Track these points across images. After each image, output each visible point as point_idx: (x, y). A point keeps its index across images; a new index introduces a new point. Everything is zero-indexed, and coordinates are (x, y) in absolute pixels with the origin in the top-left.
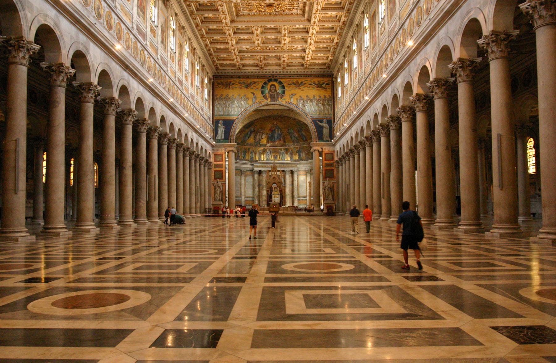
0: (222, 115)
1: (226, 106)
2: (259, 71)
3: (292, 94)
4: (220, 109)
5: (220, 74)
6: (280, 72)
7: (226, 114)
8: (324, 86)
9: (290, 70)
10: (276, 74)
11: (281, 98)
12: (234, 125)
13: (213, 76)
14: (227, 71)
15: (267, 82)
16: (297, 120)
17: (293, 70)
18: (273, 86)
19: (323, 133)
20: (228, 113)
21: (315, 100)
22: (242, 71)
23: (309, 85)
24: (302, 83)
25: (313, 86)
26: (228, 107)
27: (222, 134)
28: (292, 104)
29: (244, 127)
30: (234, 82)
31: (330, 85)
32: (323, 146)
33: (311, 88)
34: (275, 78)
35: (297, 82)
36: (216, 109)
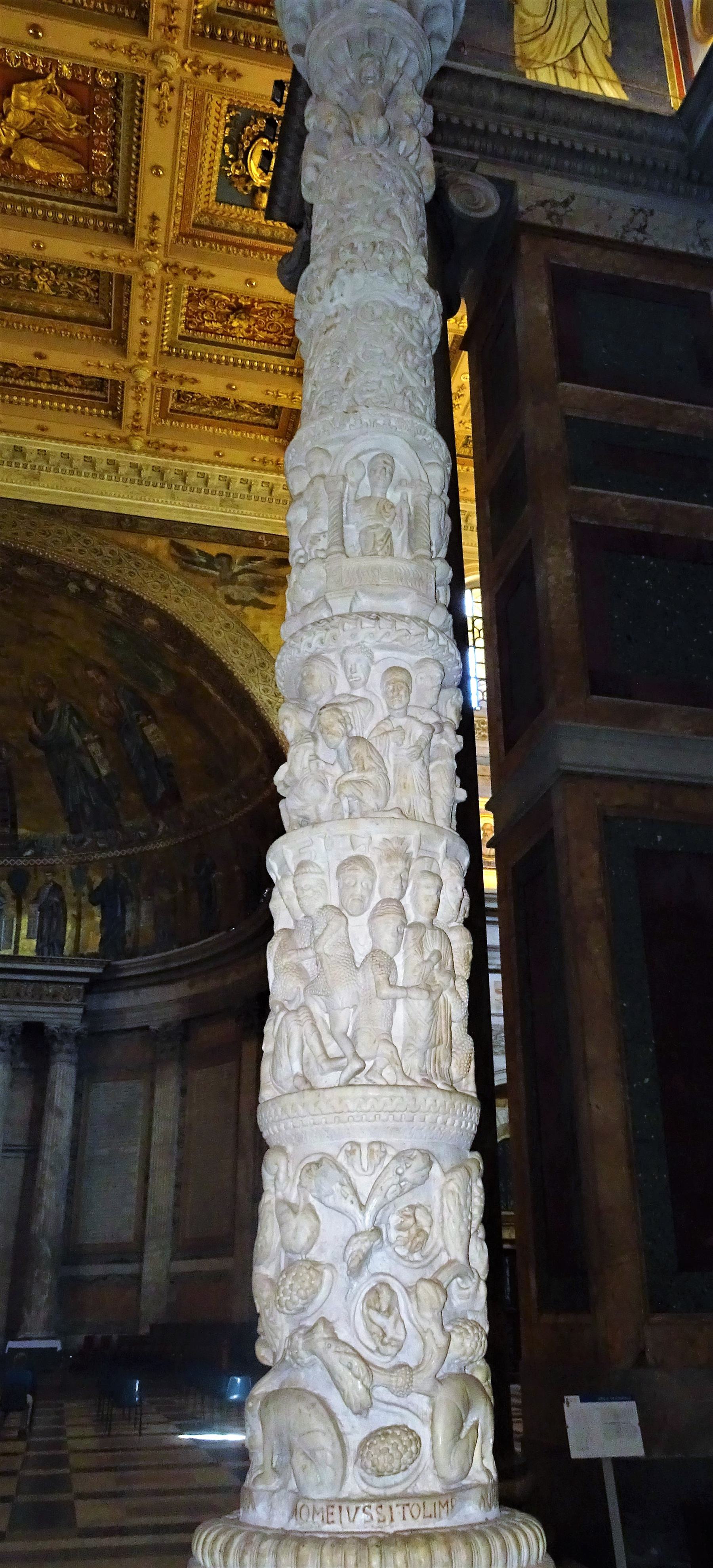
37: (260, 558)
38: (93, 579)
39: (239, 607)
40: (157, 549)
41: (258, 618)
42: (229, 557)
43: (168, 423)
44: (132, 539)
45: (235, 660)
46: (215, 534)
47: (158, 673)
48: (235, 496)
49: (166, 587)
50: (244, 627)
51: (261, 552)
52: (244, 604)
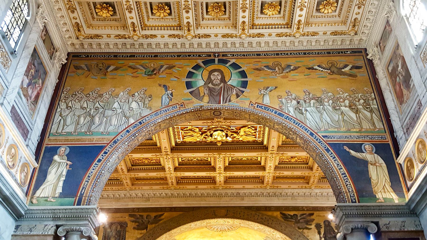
0: (70, 134)
7: (83, 131)
8: (347, 69)
11: (238, 96)
12: (100, 157)
13: (69, 54)
15: (202, 64)
18: (216, 73)
20: (90, 126)
22: (142, 40)
24: (289, 66)
27: (59, 179)
28: (267, 108)
30: (119, 66)
33: (313, 74)
34: (221, 58)
36: (57, 118)
37: (305, 214)
40: (277, 215)
42: (297, 215)
44: (270, 213)
48: (295, 196)
51: (305, 212)
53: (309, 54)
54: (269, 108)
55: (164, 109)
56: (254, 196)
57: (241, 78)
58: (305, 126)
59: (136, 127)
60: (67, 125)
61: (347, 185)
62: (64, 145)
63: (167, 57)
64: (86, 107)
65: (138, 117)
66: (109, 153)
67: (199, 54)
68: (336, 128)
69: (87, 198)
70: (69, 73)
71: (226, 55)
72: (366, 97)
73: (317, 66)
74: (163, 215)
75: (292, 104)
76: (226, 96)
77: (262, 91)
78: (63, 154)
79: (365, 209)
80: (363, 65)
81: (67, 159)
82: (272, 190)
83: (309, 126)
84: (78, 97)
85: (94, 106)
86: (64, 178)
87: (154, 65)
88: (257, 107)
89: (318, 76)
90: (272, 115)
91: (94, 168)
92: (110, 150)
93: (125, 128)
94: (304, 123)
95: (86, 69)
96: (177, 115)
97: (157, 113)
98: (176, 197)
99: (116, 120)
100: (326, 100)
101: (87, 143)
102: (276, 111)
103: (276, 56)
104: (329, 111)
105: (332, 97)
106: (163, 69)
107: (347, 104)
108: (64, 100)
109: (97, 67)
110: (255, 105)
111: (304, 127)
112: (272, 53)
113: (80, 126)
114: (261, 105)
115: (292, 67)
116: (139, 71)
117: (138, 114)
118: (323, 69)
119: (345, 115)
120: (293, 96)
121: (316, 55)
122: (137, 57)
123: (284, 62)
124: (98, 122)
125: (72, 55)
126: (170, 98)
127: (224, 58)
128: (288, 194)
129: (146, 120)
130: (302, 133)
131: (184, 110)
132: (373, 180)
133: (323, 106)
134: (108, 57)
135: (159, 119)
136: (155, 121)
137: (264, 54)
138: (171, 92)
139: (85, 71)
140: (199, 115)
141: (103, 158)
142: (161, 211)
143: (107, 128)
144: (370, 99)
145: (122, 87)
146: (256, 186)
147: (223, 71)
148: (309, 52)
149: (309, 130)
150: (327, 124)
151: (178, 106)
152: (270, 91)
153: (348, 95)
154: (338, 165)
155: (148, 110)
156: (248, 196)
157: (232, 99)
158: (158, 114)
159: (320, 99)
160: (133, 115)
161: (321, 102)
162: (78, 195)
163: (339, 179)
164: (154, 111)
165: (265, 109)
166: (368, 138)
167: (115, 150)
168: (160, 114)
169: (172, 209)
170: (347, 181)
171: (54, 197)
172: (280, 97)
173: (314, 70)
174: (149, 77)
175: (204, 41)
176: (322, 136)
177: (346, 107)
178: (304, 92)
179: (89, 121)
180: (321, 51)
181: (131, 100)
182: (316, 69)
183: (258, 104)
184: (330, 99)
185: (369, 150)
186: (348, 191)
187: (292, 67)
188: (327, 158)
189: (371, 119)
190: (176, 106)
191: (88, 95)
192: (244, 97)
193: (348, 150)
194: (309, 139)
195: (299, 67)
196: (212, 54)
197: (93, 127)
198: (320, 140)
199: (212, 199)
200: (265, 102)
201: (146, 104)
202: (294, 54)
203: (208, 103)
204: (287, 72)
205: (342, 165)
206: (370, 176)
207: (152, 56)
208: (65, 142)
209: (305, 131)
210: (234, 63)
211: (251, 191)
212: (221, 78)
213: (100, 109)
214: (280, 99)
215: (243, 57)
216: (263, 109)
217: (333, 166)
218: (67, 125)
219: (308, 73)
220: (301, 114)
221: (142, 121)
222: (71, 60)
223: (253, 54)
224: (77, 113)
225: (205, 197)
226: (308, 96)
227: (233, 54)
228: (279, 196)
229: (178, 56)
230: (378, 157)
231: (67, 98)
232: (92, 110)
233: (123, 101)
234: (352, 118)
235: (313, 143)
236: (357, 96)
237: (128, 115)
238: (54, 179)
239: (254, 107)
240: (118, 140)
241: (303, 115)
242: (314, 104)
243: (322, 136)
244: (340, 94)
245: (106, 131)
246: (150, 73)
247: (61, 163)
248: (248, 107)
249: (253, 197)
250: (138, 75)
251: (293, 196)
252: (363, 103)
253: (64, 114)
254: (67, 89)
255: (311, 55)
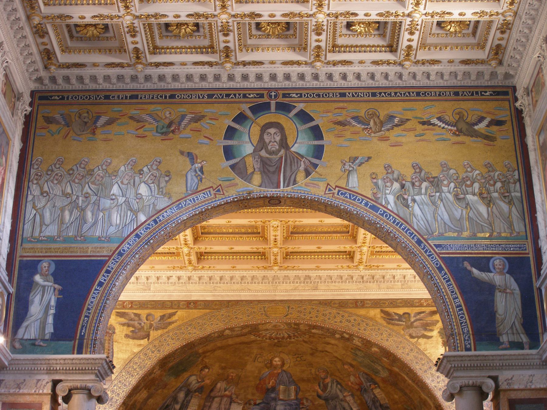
0: (51, 239)
1: (74, 205)
2: (215, 70)
3: (354, 160)
4: (47, 215)
5: (62, 85)
6: (302, 77)
7: (70, 234)
8: (481, 127)
9: (341, 69)
10: (287, 84)
11: (308, 173)
12: (100, 278)
14: (86, 72)
15: (249, 113)
16: (357, 342)
17: (356, 68)
18: (272, 131)
19: (492, 315)
20: (80, 227)
21: (450, 180)
23: (420, 128)
24: (391, 118)
25: (439, 131)
26: (83, 210)
28: (354, 195)
29: (163, 363)
31: (507, 126)
32: (501, 368)
33: (430, 134)
34: (280, 100)
35: (374, 115)
37: (423, 312)
38: (347, 334)
39: (416, 339)
40: (375, 315)
41: (425, 343)
43: (374, 256)
44: (362, 312)
45: (417, 367)
46: (401, 303)
47: (379, 368)
49: (382, 334)
50: (419, 350)
51: (423, 309)
52: (419, 337)
53: (425, 96)
54: (357, 197)
55: (190, 197)
56: (335, 282)
57: (314, 140)
58: (410, 228)
59: (150, 228)
60: (46, 223)
61: (461, 323)
62: (46, 259)
63: (191, 98)
64: (71, 192)
65: (151, 212)
66: (113, 271)
67: (244, 94)
68: (455, 231)
69: (90, 343)
70: (37, 130)
71: (289, 94)
72: (507, 177)
73: (437, 118)
74: (174, 314)
75: (393, 188)
76: (288, 174)
77: (347, 164)
78: (47, 273)
79: (481, 360)
80: (508, 118)
81: (54, 281)
82: (368, 272)
83: (416, 227)
84: (57, 175)
85: (82, 191)
86: (52, 311)
87: (170, 113)
88: (338, 194)
89: (437, 137)
90: (361, 208)
91: (95, 296)
92: (115, 267)
93: (132, 230)
94: (409, 223)
95: (63, 123)
96: (212, 208)
97: (180, 204)
98: (196, 283)
99: (118, 216)
100: (445, 182)
101: (79, 254)
102: (367, 202)
103: (371, 98)
104: (449, 202)
105: (455, 178)
106: (185, 122)
107: (477, 190)
108: (36, 180)
109: (79, 118)
110: (334, 191)
111: (408, 229)
112: (366, 91)
113: (65, 226)
114: (344, 191)
115: (396, 120)
116: (147, 126)
117: (151, 206)
118: (446, 124)
119: (471, 208)
120: (395, 176)
121: (435, 98)
122: (141, 98)
123: (384, 111)
124: (91, 220)
125: (37, 95)
126: (199, 178)
127: (286, 100)
128: (396, 278)
129: (163, 216)
130: (406, 240)
131: (222, 199)
132: (500, 315)
133: (441, 193)
134: (96, 99)
135: (183, 214)
136: (177, 218)
137: (352, 94)
138: (200, 165)
139: (62, 126)
140: (246, 204)
141: (105, 280)
142: (171, 307)
143: (105, 231)
144: (511, 181)
145: (122, 156)
146: (340, 266)
147: (284, 126)
148: (426, 90)
149: (415, 235)
150: (443, 225)
151: (212, 192)
152: (359, 166)
153: (479, 174)
154: (453, 292)
155: (166, 199)
156: (325, 282)
157: (298, 179)
158: (182, 206)
159: (436, 179)
160: (143, 206)
161: (438, 186)
162: (78, 338)
163: (452, 313)
164: (174, 201)
165: (350, 198)
166: (500, 249)
167: (121, 267)
168: (185, 205)
169: (190, 304)
170: (462, 317)
171: (43, 340)
172: (374, 176)
173: (431, 127)
174: (163, 137)
175: (252, 70)
176: (435, 245)
177: (474, 194)
178: (413, 167)
179: (77, 218)
180: (445, 90)
181: (137, 179)
182: (434, 125)
183: (340, 189)
184: (452, 180)
185: (499, 268)
186: (461, 333)
187: (396, 120)
188: (438, 281)
189: (508, 215)
190: (209, 191)
191: (71, 172)
192: (317, 176)
193: (469, 268)
194: (415, 249)
195: (408, 120)
196: (265, 93)
197: (85, 227)
198: (430, 252)
199: (261, 287)
200: (350, 186)
201: (162, 188)
202: (401, 94)
203: (260, 186)
204: (388, 130)
205: (458, 293)
206: (495, 309)
207: (166, 97)
208: (46, 252)
209: (409, 237)
210: (302, 110)
211: (331, 273)
212: (281, 140)
213: (92, 197)
214: (375, 181)
215: (317, 99)
216: (346, 197)
217: (445, 294)
218: (46, 225)
219: (422, 132)
220: (406, 207)
221: (158, 218)
222: (38, 106)
223: (333, 93)
224: (59, 204)
225: (248, 283)
226: (418, 175)
227: (302, 93)
228: (380, 282)
229: (210, 96)
230: (510, 279)
231: (40, 176)
232: (81, 198)
233: (126, 182)
234: (480, 214)
235: (420, 257)
236: (492, 176)
237: (136, 207)
238: (39, 313)
239: (333, 193)
240: (124, 250)
241: (408, 208)
242: (426, 189)
243: (435, 245)
244: (467, 171)
245: (105, 234)
246: (164, 130)
247: (47, 287)
248: (323, 193)
249: (333, 284)
250: (146, 133)
251: (405, 281)
252: (500, 189)
253: (39, 205)
254: (37, 160)
255: (428, 98)
